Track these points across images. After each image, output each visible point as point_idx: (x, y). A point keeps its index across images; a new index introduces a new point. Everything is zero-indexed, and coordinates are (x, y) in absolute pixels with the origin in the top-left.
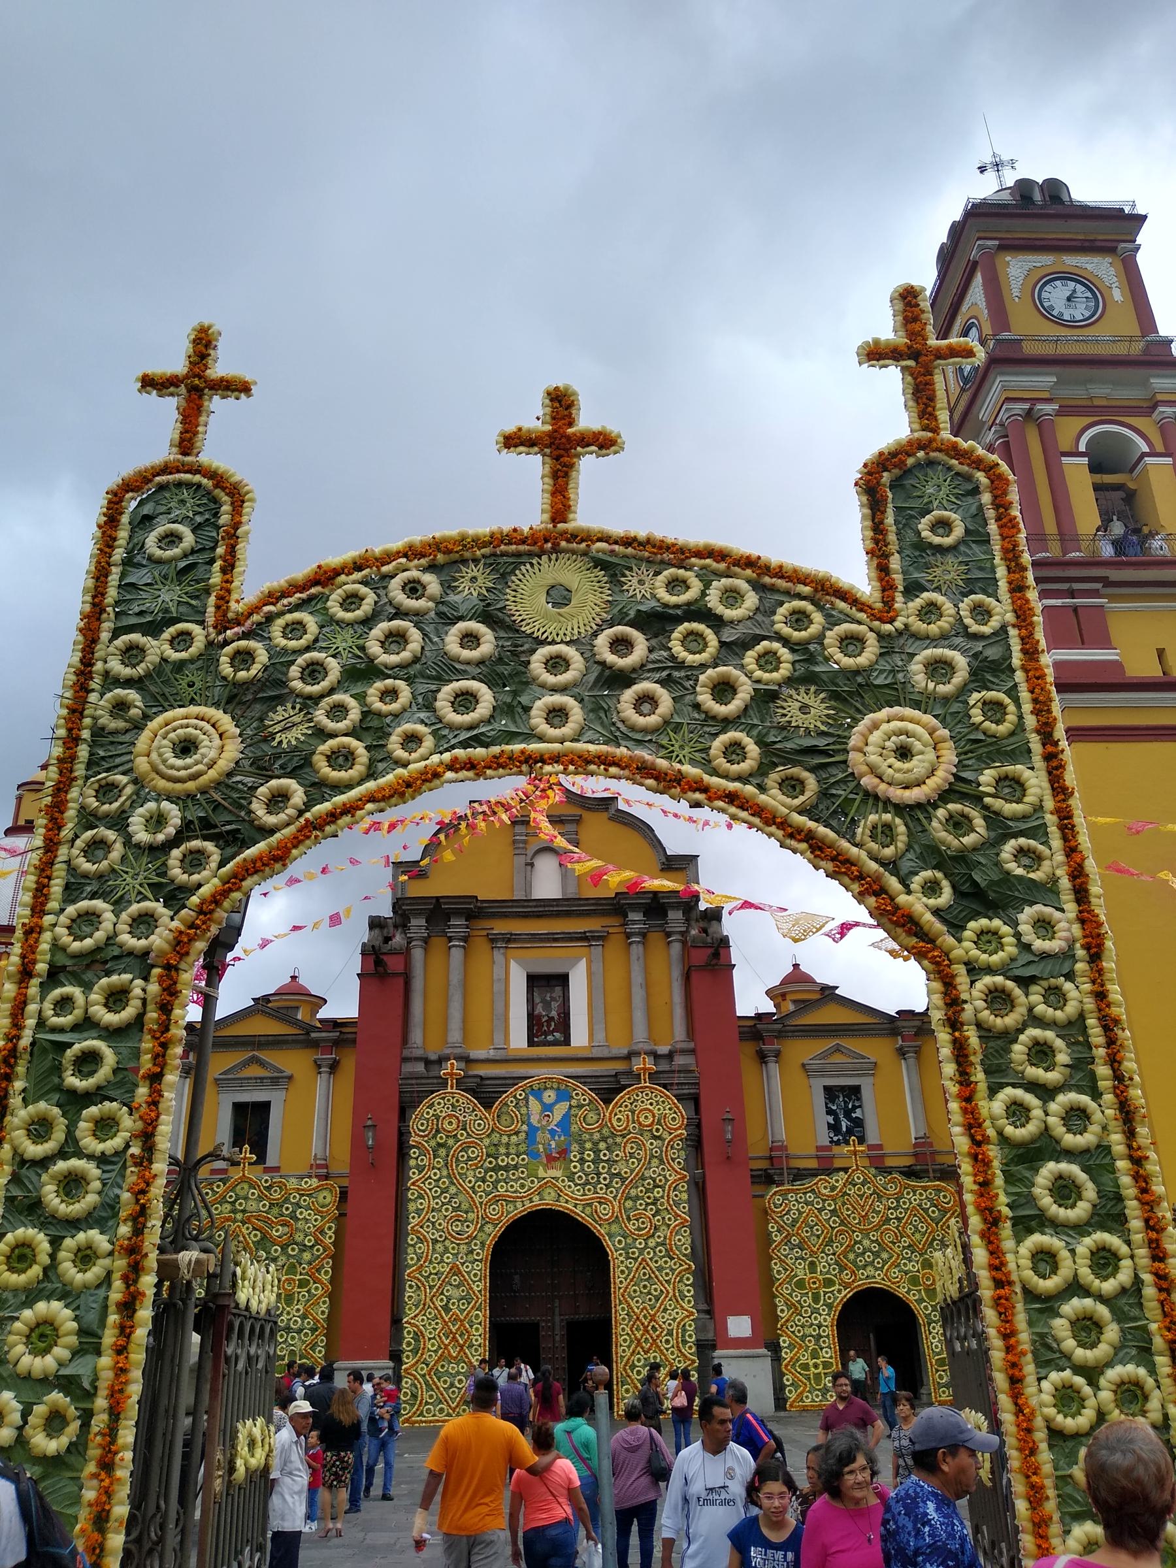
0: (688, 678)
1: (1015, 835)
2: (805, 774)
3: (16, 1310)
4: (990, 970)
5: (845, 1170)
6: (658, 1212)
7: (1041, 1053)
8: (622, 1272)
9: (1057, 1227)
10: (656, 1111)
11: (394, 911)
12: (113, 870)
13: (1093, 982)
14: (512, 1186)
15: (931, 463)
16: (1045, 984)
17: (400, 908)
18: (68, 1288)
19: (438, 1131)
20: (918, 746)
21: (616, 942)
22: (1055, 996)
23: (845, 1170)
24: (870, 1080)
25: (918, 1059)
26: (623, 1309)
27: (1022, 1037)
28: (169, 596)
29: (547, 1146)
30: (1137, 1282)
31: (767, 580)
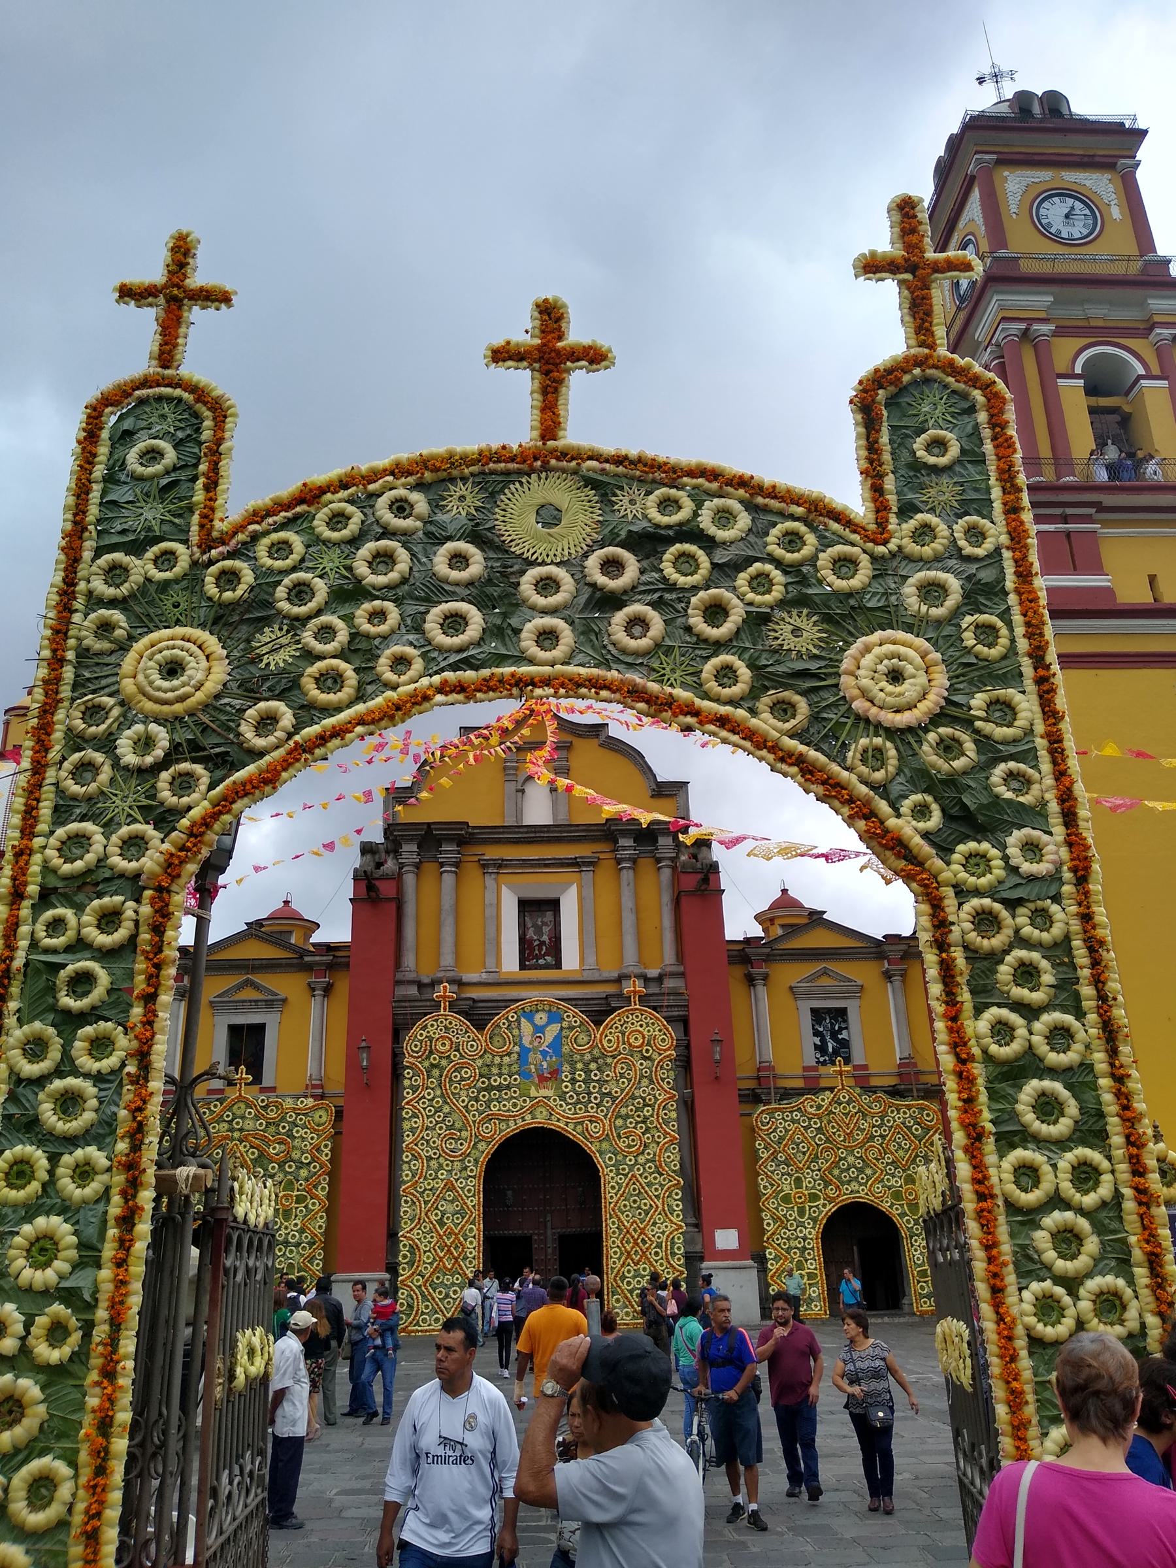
0: (680, 600)
1: (1005, 759)
2: (797, 698)
3: (16, 1225)
4: (977, 892)
5: (831, 1089)
6: (647, 1130)
7: (1027, 974)
8: (613, 1187)
9: (1040, 1142)
10: (645, 1033)
11: (386, 838)
12: (102, 792)
13: (1080, 904)
14: (505, 1106)
15: (927, 381)
16: (1032, 906)
17: (392, 834)
18: (68, 1203)
19: (431, 1052)
20: (909, 669)
21: (606, 867)
22: (1042, 918)
23: (831, 1089)
24: (856, 1002)
25: (904, 982)
26: (613, 1223)
27: (1008, 958)
28: (152, 514)
29: (539, 1067)
30: (1118, 1196)
31: (760, 500)
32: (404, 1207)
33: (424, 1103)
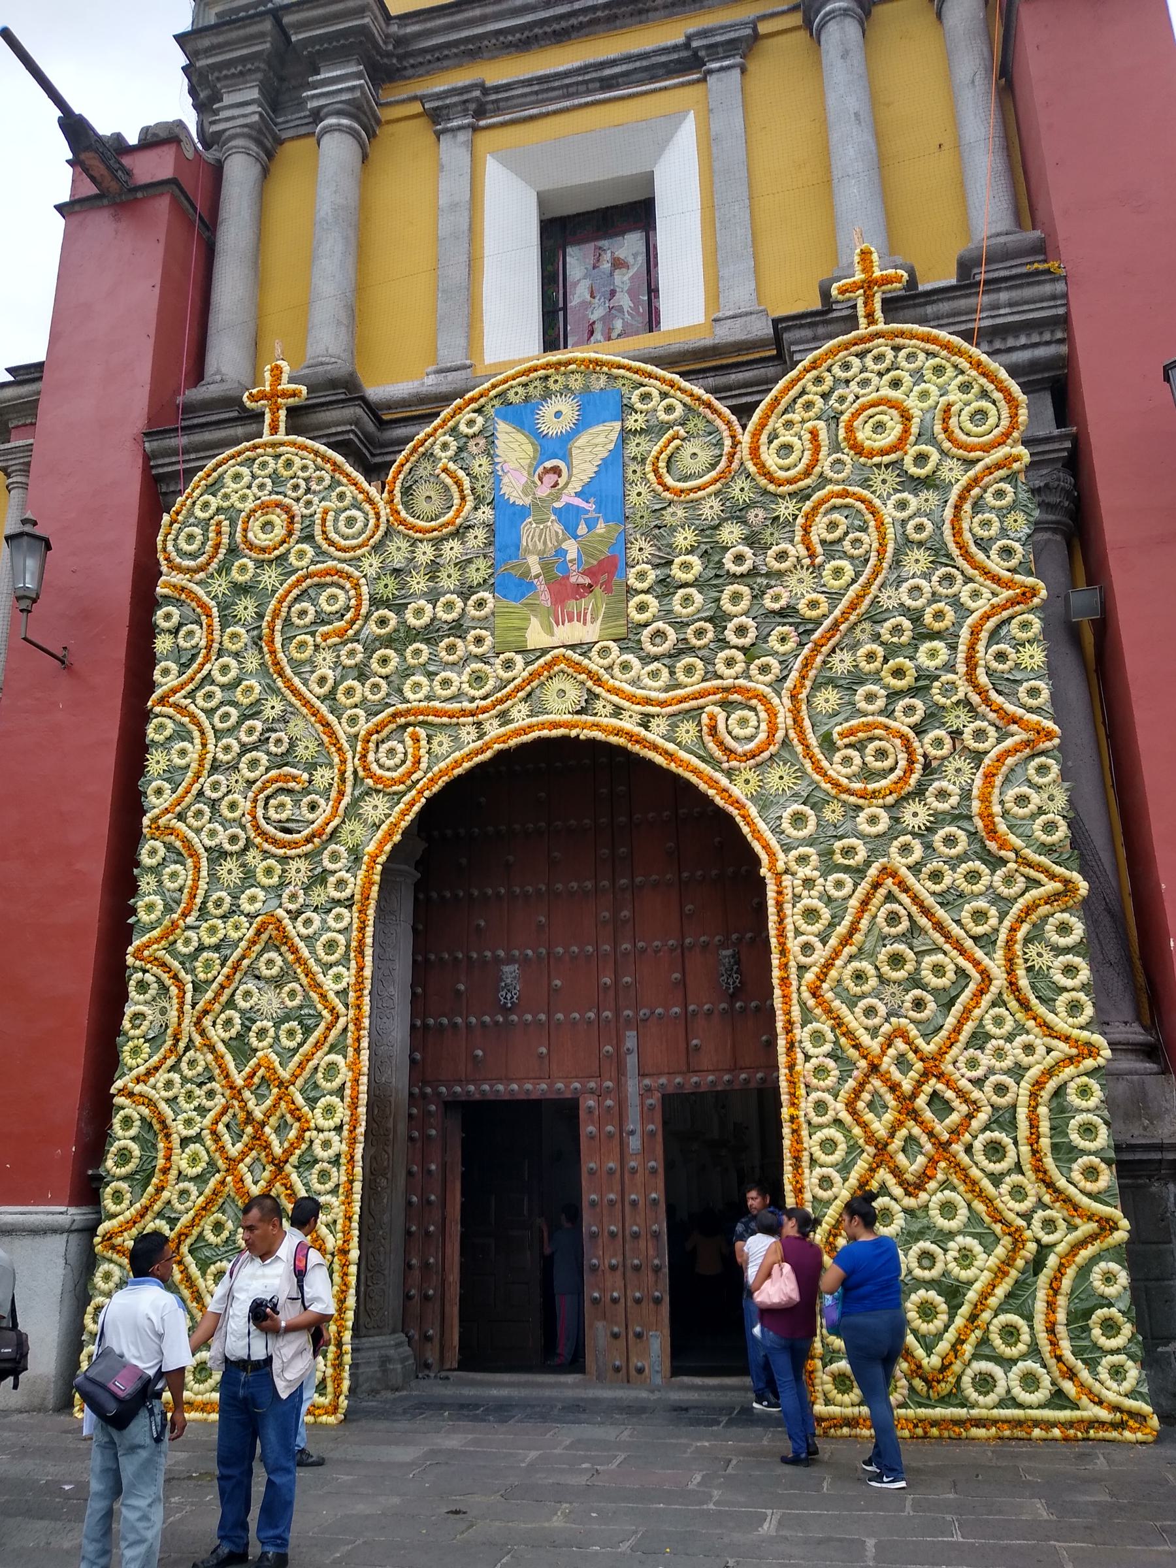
6: (934, 715)
19: (233, 551)
26: (818, 1037)
29: (553, 563)
32: (136, 1003)
33: (209, 696)
